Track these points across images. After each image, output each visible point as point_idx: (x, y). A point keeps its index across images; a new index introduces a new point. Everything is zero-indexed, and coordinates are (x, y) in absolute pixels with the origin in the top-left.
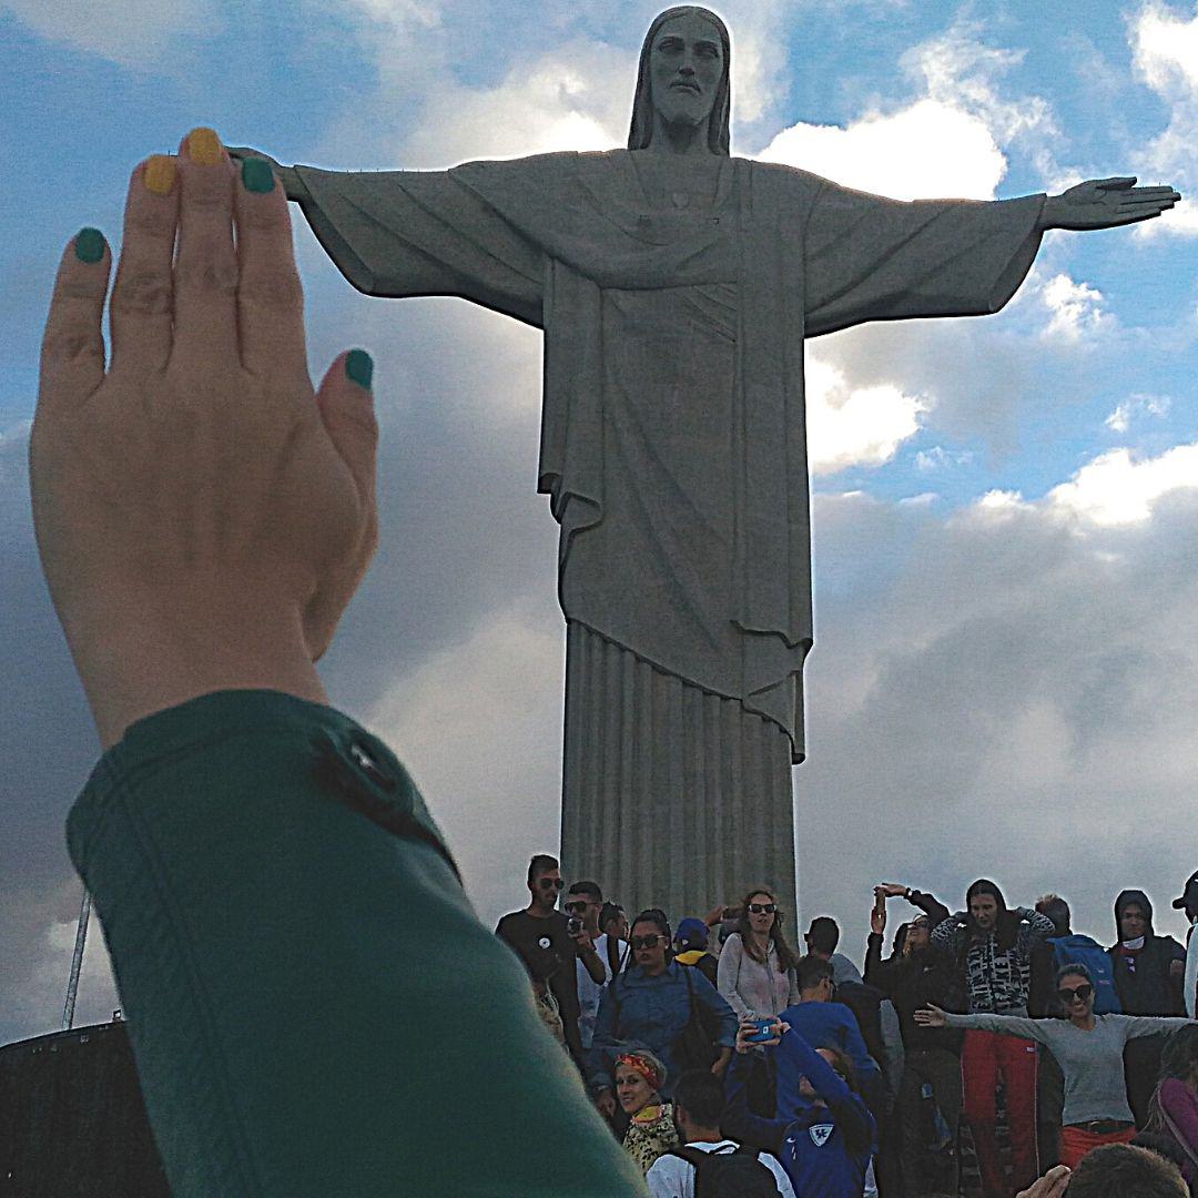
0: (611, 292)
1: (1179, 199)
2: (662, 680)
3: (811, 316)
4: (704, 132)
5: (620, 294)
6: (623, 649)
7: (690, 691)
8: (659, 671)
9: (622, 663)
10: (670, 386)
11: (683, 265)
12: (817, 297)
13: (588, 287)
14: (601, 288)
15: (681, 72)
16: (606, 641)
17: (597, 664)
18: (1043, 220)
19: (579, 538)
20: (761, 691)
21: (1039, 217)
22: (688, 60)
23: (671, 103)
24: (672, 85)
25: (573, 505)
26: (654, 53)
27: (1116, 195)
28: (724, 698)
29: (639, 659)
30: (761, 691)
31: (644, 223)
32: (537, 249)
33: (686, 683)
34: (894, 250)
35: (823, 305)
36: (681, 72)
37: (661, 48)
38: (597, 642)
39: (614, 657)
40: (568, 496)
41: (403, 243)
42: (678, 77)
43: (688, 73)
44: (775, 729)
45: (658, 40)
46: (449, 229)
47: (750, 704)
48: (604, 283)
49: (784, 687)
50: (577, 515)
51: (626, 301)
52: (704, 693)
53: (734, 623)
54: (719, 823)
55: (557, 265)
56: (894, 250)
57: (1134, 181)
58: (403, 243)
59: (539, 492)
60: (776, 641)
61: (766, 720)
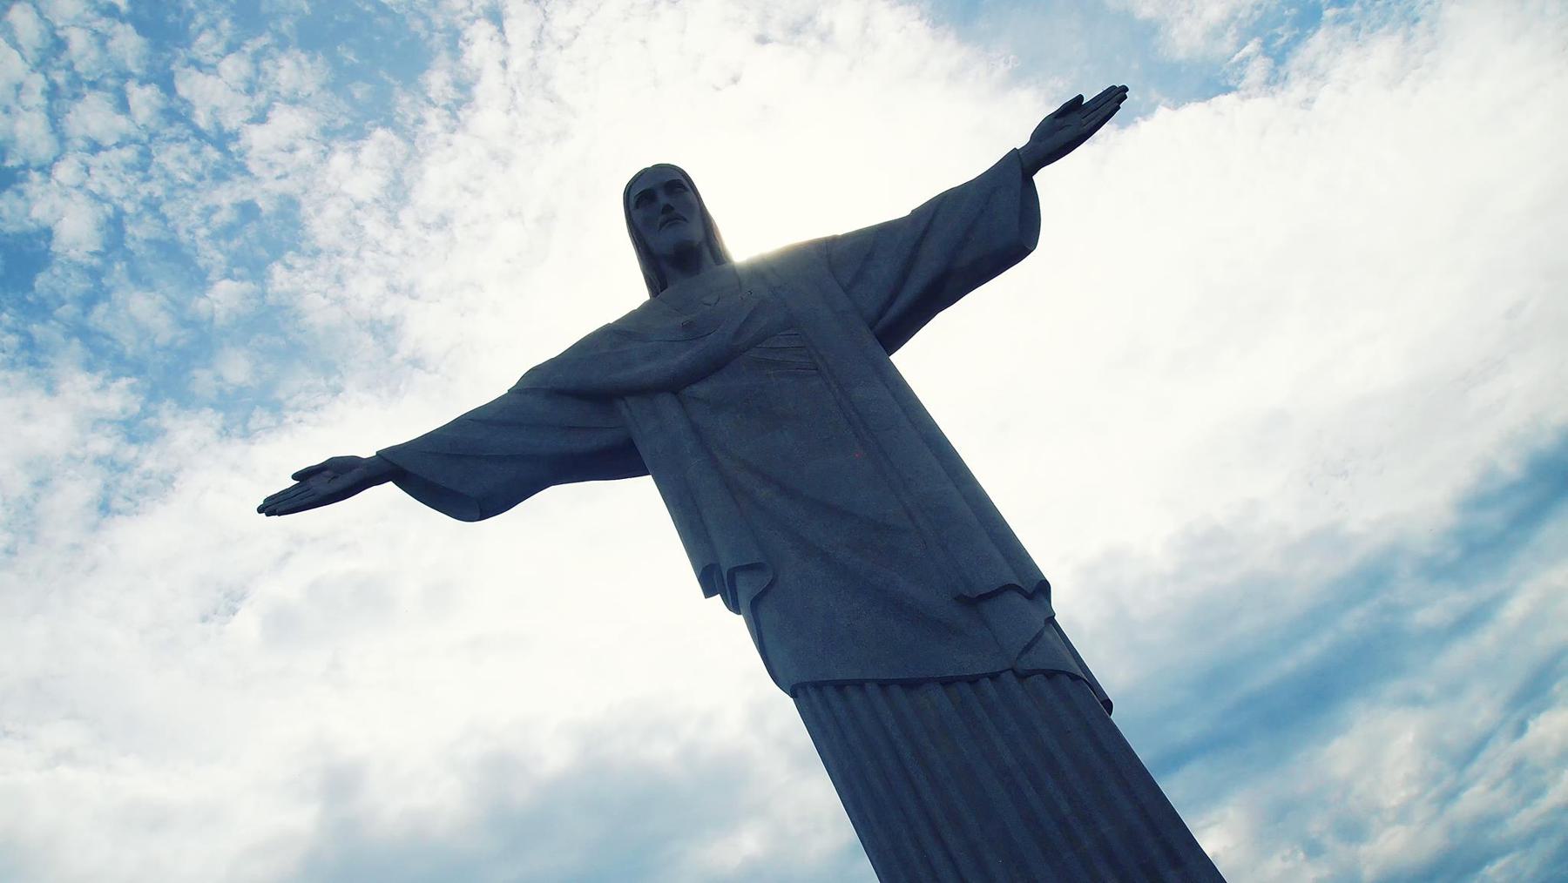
0: (687, 391)
1: (1125, 89)
5: (695, 387)
6: (860, 685)
8: (910, 685)
11: (738, 333)
13: (666, 402)
14: (675, 393)
15: (663, 212)
16: (840, 686)
22: (663, 199)
23: (664, 241)
24: (662, 225)
25: (741, 579)
26: (634, 213)
27: (1075, 116)
28: (994, 677)
29: (883, 685)
31: (687, 327)
33: (947, 683)
34: (918, 245)
35: (880, 316)
36: (663, 212)
37: (637, 206)
38: (830, 693)
39: (855, 697)
40: (732, 573)
42: (662, 218)
43: (668, 209)
45: (633, 201)
47: (1025, 665)
48: (674, 386)
49: (1047, 634)
51: (701, 390)
52: (970, 683)
54: (1065, 808)
55: (630, 401)
56: (918, 245)
57: (1080, 98)
61: (1051, 675)
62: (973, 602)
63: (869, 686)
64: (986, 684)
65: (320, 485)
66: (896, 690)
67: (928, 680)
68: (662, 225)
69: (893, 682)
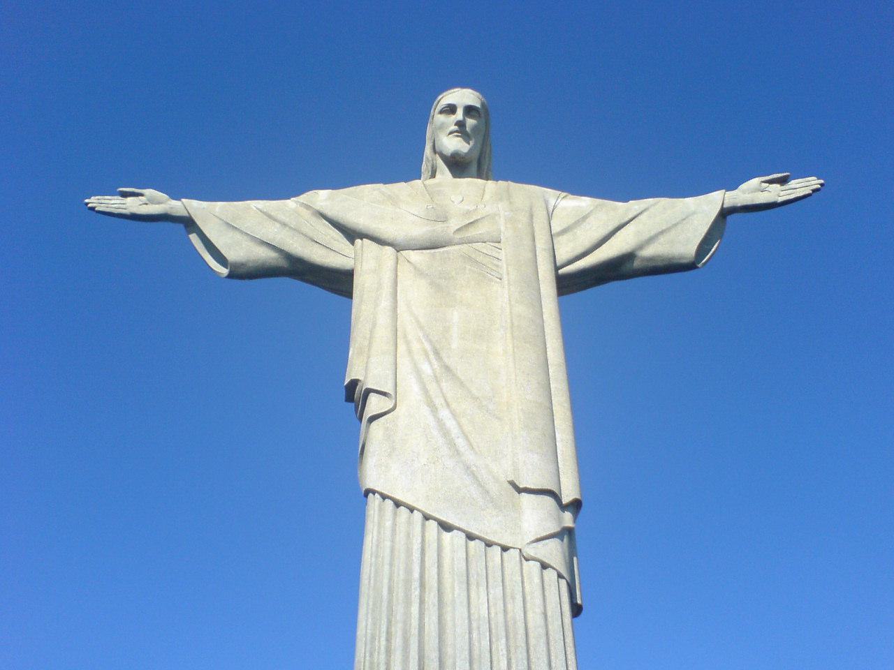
2: (447, 536)
3: (561, 271)
4: (474, 168)
6: (412, 510)
7: (472, 544)
8: (446, 527)
9: (409, 523)
10: (452, 309)
12: (562, 256)
17: (388, 524)
18: (725, 206)
19: (375, 424)
20: (538, 540)
21: (723, 204)
24: (451, 133)
25: (373, 400)
28: (505, 549)
29: (427, 518)
30: (538, 540)
32: (352, 234)
38: (389, 503)
41: (254, 239)
44: (550, 575)
46: (287, 228)
47: (530, 551)
48: (398, 247)
50: (375, 405)
51: (414, 256)
53: (513, 484)
58: (254, 239)
59: (346, 401)
60: (549, 500)
61: (544, 566)
62: (520, 490)
63: (415, 511)
64: (496, 550)
65: (132, 205)
66: (432, 525)
67: (459, 529)
68: (451, 133)
69: (435, 519)
